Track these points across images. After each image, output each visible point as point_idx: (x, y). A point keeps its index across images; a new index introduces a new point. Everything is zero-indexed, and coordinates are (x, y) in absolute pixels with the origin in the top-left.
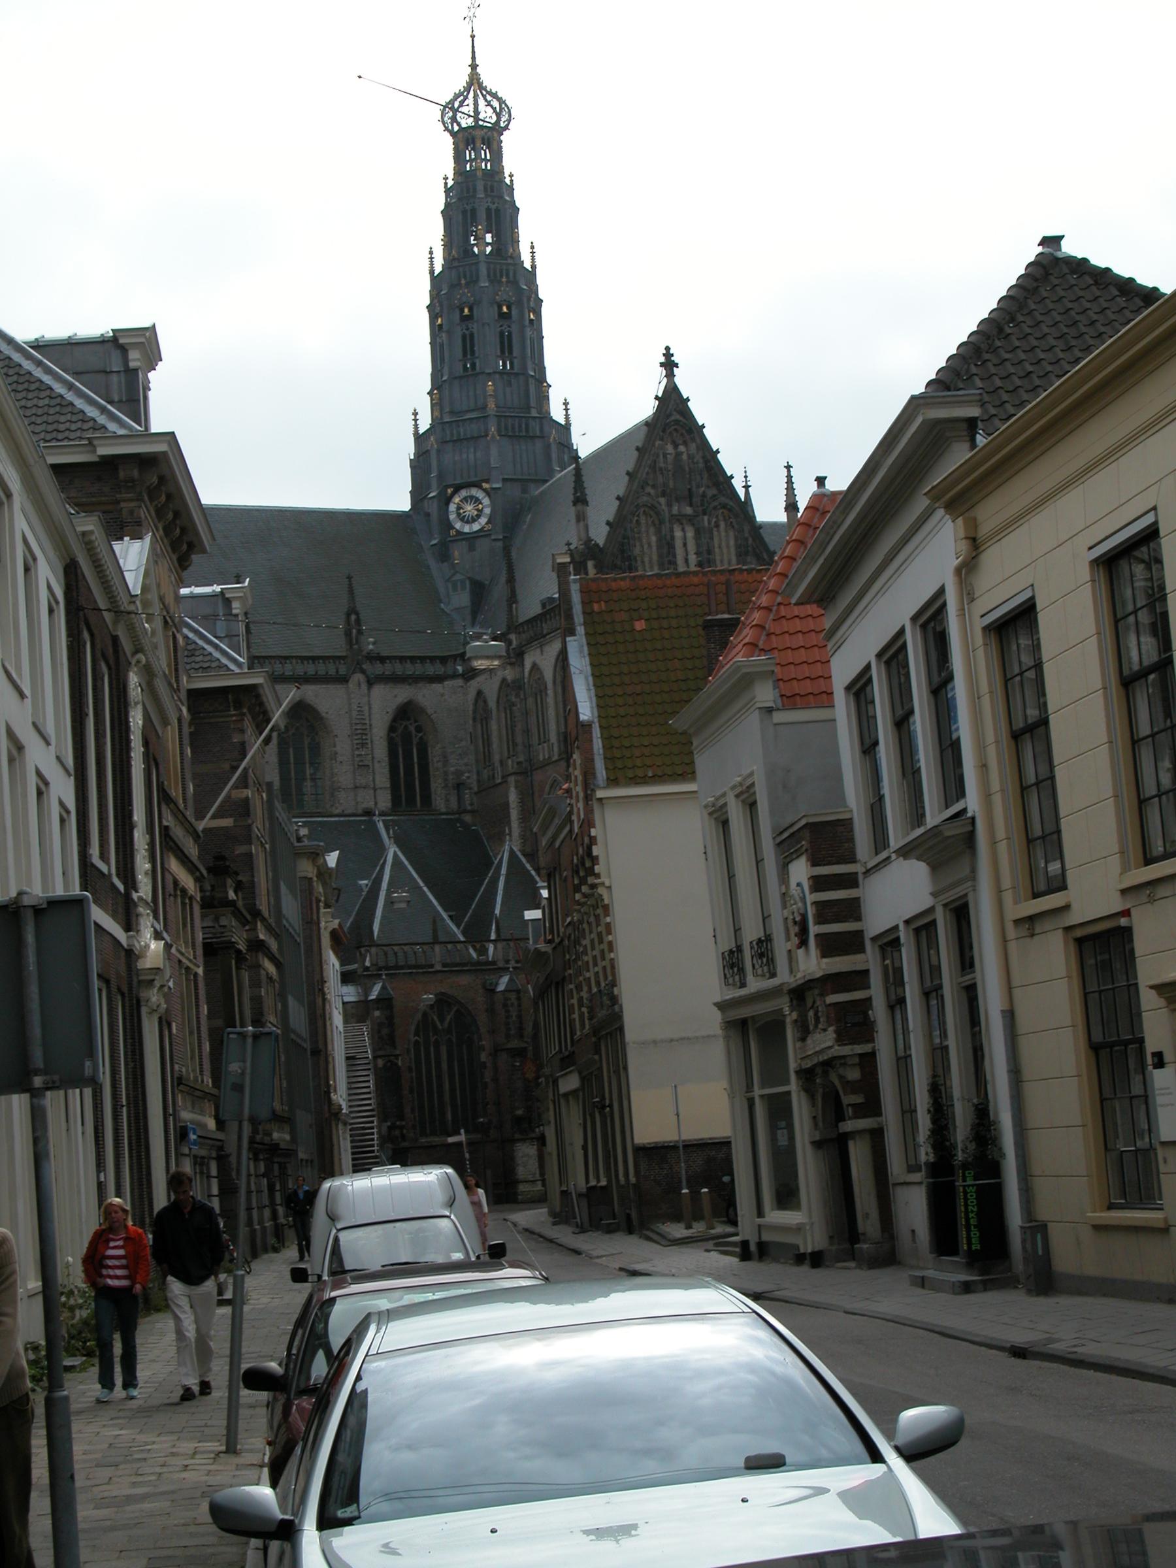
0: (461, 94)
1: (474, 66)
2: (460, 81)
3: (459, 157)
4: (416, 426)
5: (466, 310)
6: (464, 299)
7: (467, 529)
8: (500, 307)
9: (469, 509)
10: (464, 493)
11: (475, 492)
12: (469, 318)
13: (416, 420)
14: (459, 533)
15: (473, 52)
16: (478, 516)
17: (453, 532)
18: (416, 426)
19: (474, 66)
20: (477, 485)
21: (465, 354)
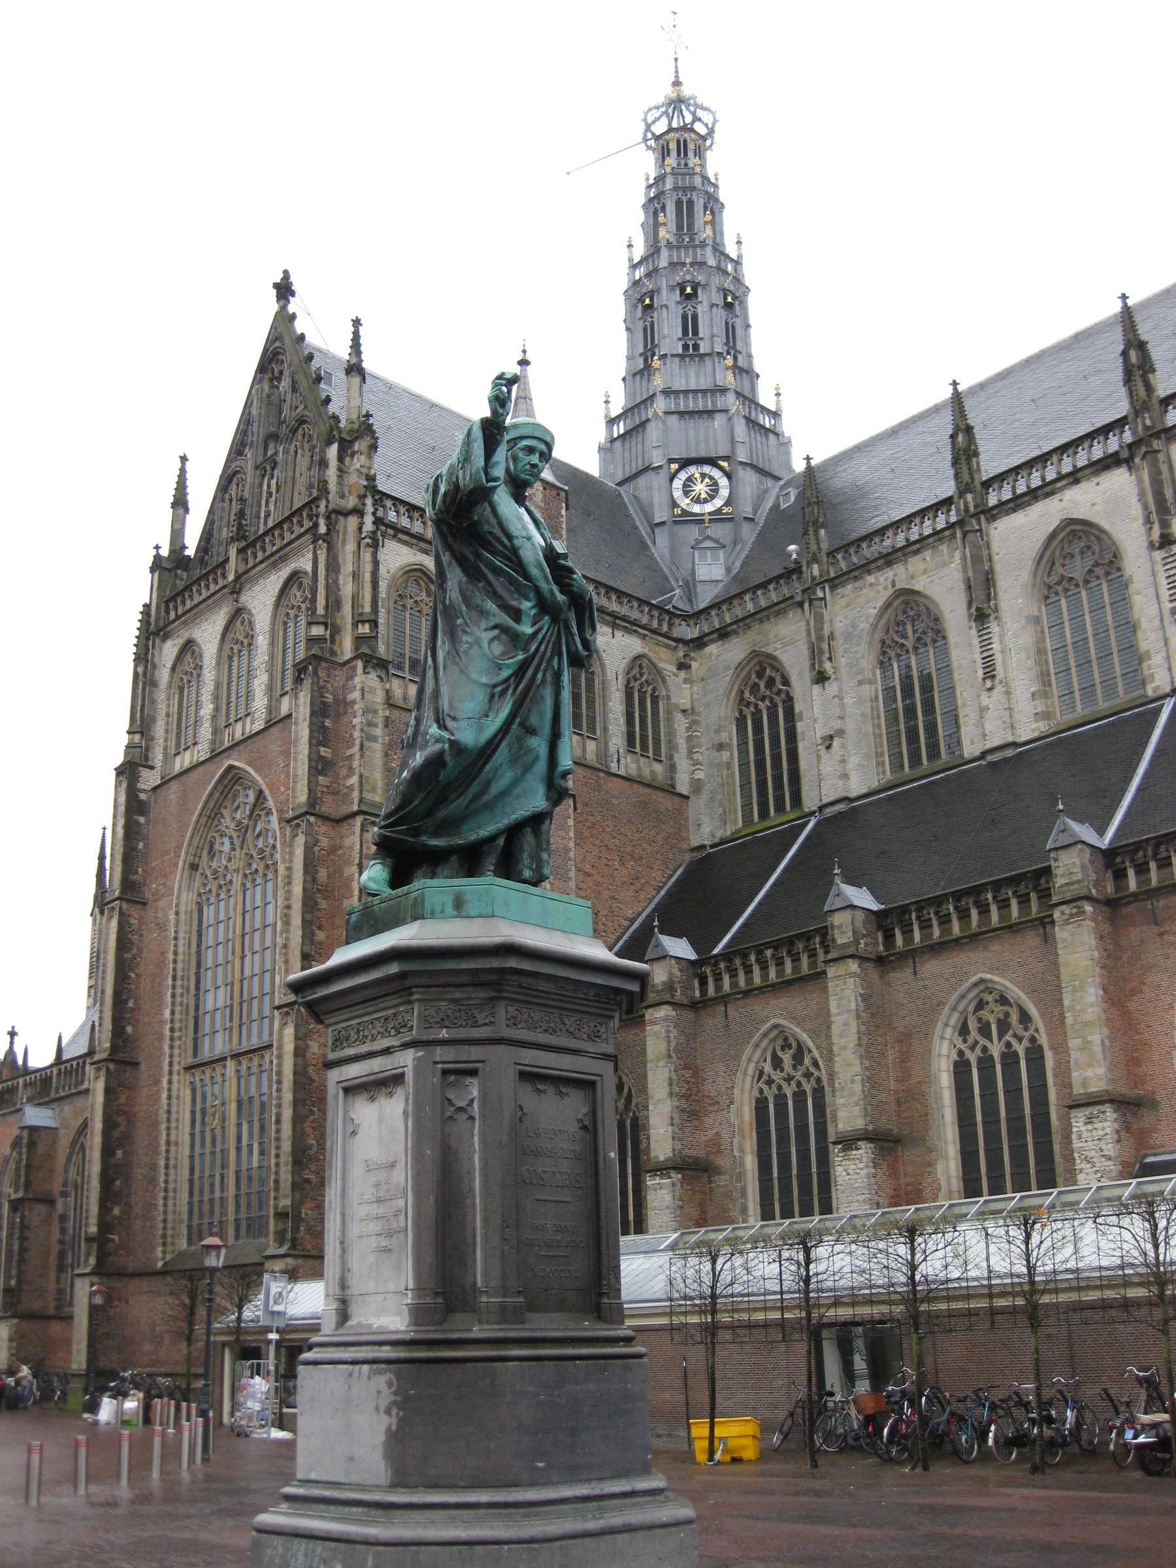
1: (677, 83)
2: (668, 91)
3: (664, 152)
4: (607, 409)
5: (689, 290)
6: (688, 277)
7: (696, 509)
8: (725, 298)
9: (701, 488)
10: (692, 470)
11: (707, 469)
12: (688, 297)
13: (607, 402)
14: (685, 513)
15: (677, 72)
16: (712, 497)
17: (678, 511)
18: (607, 409)
19: (677, 83)
20: (712, 462)
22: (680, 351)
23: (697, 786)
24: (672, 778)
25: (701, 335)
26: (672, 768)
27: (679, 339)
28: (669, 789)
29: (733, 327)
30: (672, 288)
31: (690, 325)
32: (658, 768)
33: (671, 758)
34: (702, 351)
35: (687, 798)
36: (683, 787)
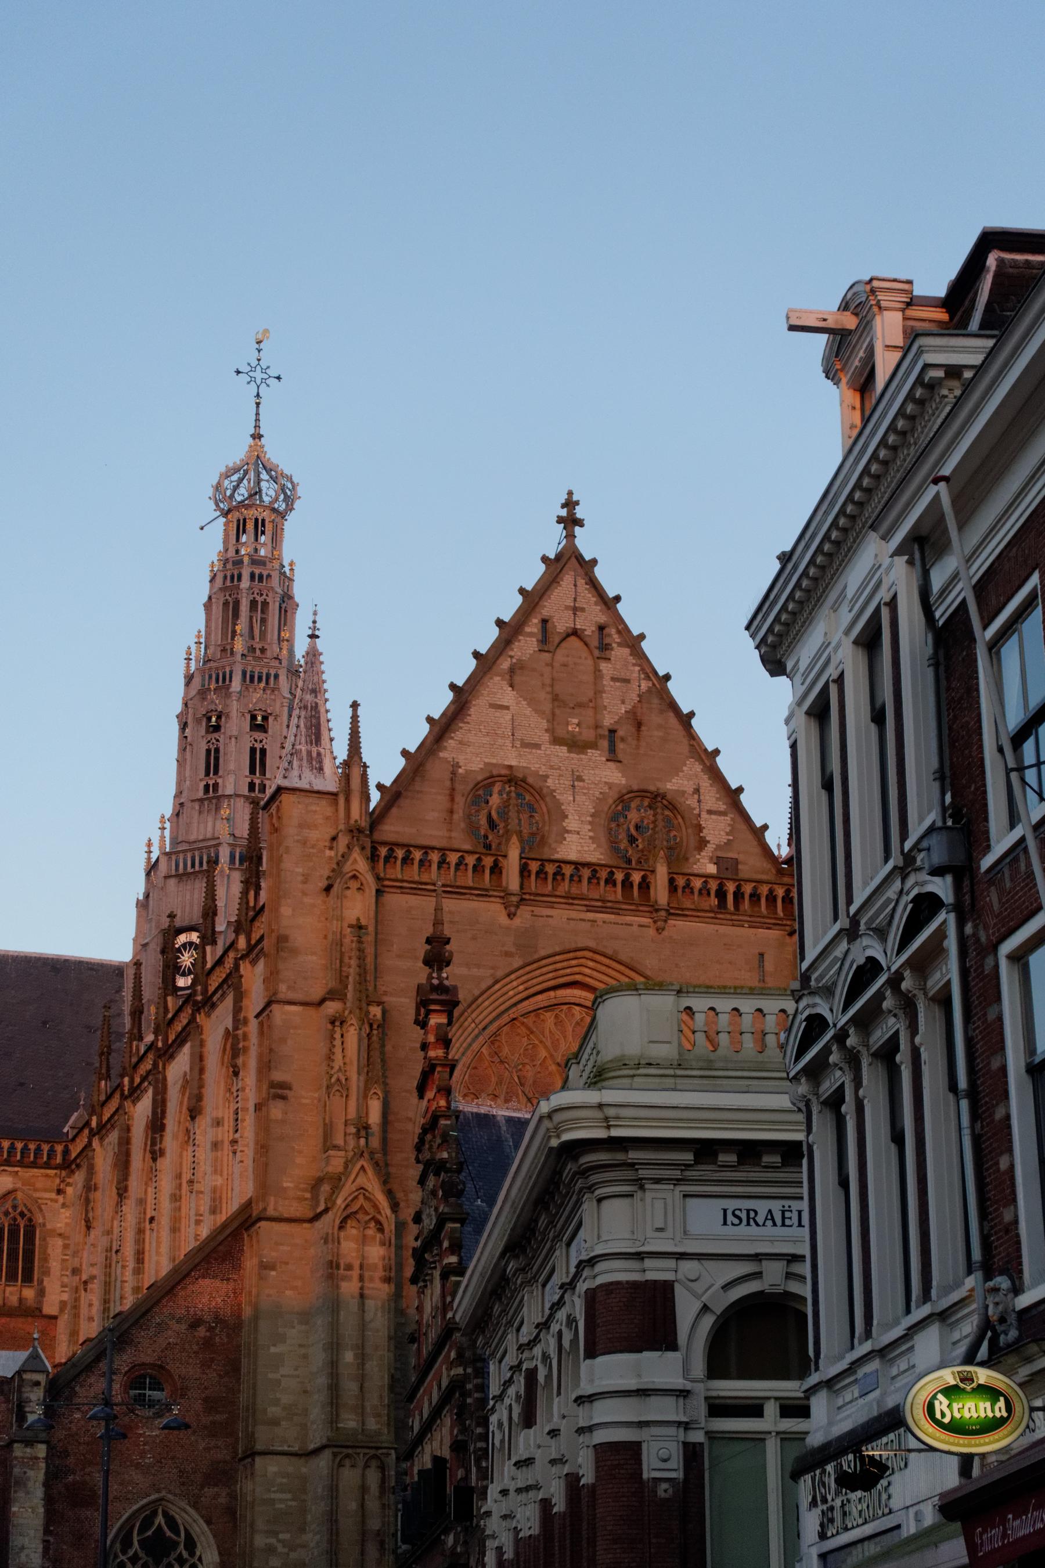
0: (236, 470)
1: (257, 436)
5: (214, 719)
6: (213, 707)
8: (254, 717)
15: (257, 420)
18: (149, 859)
19: (257, 436)
21: (207, 774)
22: (201, 794)
23: (63, 1305)
24: (41, 1302)
25: (221, 773)
26: (41, 1293)
27: (201, 780)
28: (34, 1312)
29: (263, 751)
30: (198, 721)
31: (213, 762)
32: (29, 1293)
33: (41, 1282)
34: (220, 793)
35: (55, 1318)
36: (49, 1309)
